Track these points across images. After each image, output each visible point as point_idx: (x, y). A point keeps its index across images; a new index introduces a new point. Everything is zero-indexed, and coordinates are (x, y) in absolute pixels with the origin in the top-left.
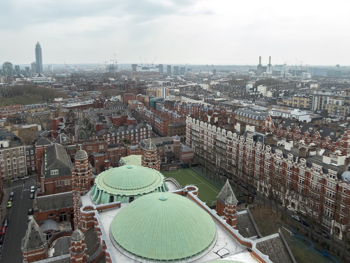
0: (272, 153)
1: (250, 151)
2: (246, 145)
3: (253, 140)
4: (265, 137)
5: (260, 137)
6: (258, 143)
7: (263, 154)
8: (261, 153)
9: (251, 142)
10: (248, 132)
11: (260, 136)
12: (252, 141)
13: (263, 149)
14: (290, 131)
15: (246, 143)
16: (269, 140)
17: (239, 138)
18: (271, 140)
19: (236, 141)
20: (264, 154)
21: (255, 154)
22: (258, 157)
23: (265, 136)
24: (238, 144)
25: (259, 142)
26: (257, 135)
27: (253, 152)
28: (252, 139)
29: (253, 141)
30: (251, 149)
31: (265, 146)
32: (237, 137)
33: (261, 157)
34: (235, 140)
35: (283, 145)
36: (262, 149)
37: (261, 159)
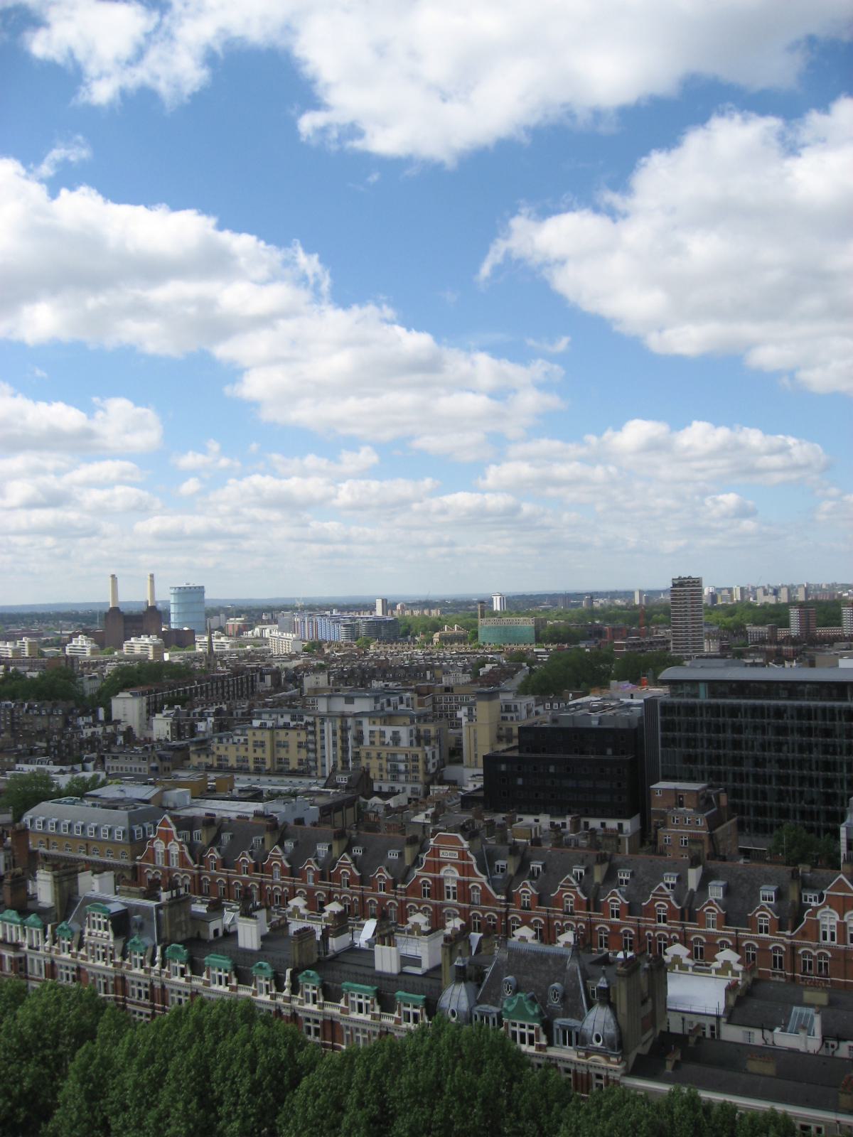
0: (193, 973)
1: (105, 985)
2: (84, 958)
3: (110, 933)
4: (161, 912)
5: (136, 917)
6: (134, 943)
7: (157, 985)
8: (152, 984)
9: (105, 944)
10: (89, 900)
11: (138, 909)
12: (108, 938)
13: (157, 967)
14: (251, 868)
15: (83, 952)
16: (177, 920)
17: (53, 932)
18: (183, 918)
19: (41, 952)
20: (163, 987)
21: (125, 993)
22: (138, 1004)
23: (158, 907)
24: (48, 961)
25: (135, 939)
26: (126, 910)
27: (119, 983)
28: (106, 929)
29: (111, 940)
30: (107, 974)
31: (163, 950)
32: (45, 933)
33: (153, 1000)
34: (37, 949)
35: (232, 929)
36: (153, 963)
37: (153, 1007)
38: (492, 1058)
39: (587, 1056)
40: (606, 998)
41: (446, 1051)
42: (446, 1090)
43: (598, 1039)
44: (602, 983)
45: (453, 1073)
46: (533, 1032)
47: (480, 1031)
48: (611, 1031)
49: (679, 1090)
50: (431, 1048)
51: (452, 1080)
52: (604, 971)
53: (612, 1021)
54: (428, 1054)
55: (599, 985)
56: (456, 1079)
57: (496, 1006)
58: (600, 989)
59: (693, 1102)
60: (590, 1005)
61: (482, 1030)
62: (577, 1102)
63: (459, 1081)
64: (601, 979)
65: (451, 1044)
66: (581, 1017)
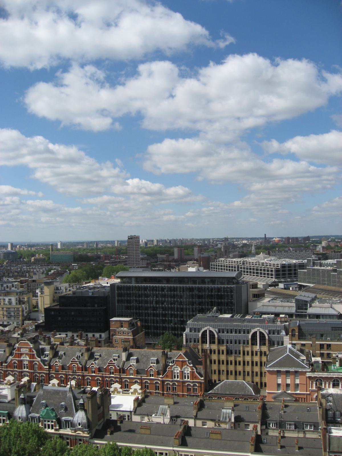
38: (33, 436)
39: (75, 431)
40: (82, 407)
41: (13, 435)
42: (13, 452)
43: (79, 425)
44: (81, 401)
45: (16, 444)
46: (53, 423)
47: (28, 425)
48: (85, 421)
49: (109, 443)
50: (7, 434)
51: (15, 447)
52: (82, 396)
53: (85, 417)
54: (5, 437)
55: (80, 402)
56: (17, 447)
57: (38, 414)
58: (80, 404)
59: (115, 448)
60: (77, 411)
61: (30, 424)
62: (69, 452)
63: (18, 447)
64: (81, 400)
65: (16, 432)
66: (73, 416)
